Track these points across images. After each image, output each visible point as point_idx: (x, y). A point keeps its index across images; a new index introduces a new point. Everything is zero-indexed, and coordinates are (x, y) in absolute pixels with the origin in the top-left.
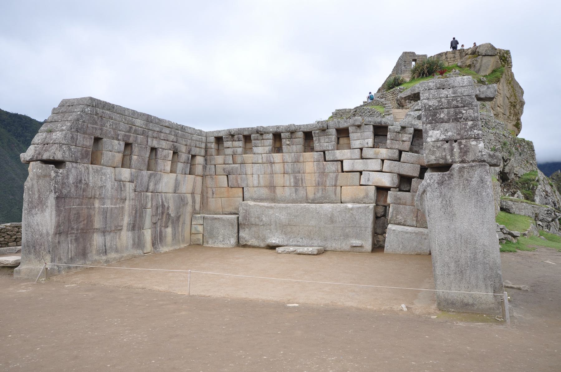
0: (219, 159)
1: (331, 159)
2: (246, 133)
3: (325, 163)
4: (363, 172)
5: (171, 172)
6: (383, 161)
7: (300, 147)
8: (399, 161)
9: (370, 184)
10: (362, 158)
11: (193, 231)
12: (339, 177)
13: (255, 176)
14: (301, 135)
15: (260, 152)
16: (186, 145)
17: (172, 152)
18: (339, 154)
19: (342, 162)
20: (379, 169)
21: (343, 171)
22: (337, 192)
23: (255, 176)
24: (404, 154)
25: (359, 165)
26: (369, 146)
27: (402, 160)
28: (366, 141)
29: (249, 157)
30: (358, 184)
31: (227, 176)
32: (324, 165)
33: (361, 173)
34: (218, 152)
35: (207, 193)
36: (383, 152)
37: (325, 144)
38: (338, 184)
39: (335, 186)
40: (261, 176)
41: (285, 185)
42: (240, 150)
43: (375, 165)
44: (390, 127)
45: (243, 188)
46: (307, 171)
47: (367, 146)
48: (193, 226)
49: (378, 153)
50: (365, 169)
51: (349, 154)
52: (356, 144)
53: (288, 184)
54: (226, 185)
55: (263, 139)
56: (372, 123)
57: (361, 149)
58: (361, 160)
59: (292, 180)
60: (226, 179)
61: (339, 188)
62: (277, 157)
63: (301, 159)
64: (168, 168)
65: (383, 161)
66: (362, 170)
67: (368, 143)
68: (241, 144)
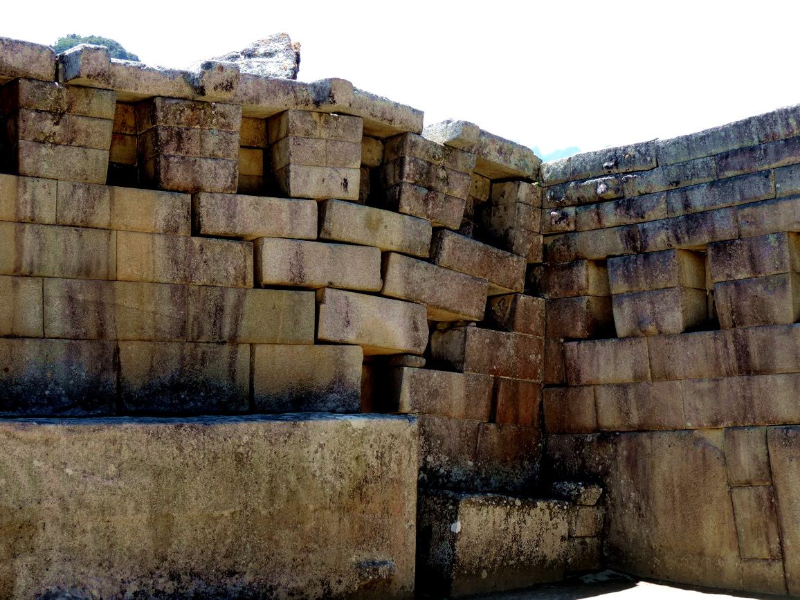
1: (222, 228)
3: (197, 241)
4: (328, 291)
6: (385, 255)
7: (97, 160)
8: (432, 259)
9: (351, 338)
14: (105, 106)
18: (254, 213)
19: (256, 247)
20: (375, 284)
21: (258, 284)
22: (238, 367)
24: (449, 241)
25: (319, 265)
27: (444, 256)
28: (344, 173)
32: (190, 251)
36: (394, 229)
37: (207, 164)
38: (243, 333)
39: (234, 340)
41: (19, 330)
43: (361, 270)
44: (413, 138)
46: (125, 271)
47: (342, 195)
49: (380, 221)
50: (337, 282)
51: (285, 216)
52: (307, 178)
53: (31, 321)
56: (363, 113)
58: (322, 247)
59: (57, 307)
61: (244, 351)
63: (101, 216)
65: (385, 255)
66: (326, 283)
67: (345, 183)
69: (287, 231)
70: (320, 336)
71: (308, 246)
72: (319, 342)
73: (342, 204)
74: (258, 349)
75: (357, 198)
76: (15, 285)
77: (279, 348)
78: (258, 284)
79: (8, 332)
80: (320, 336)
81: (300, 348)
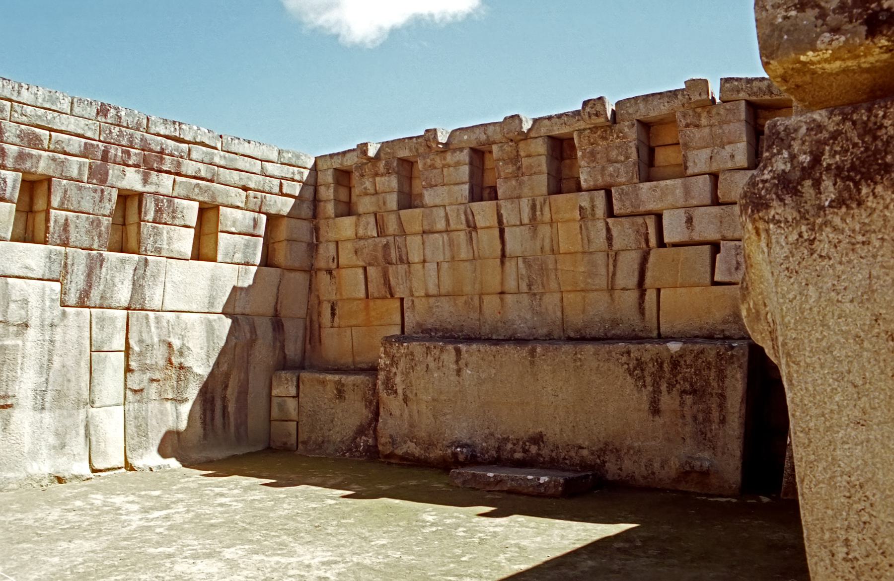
0: (346, 226)
2: (404, 153)
5: (197, 256)
7: (542, 182)
10: (716, 202)
11: (275, 413)
12: (652, 259)
13: (431, 267)
14: (540, 147)
15: (438, 201)
16: (245, 189)
17: (196, 205)
18: (649, 195)
19: (659, 217)
21: (661, 244)
23: (431, 267)
26: (738, 165)
29: (413, 217)
30: (708, 280)
31: (365, 269)
33: (715, 247)
34: (347, 209)
35: (319, 314)
40: (445, 266)
42: (392, 201)
45: (402, 300)
47: (730, 165)
48: (275, 401)
51: (679, 192)
52: (699, 160)
54: (362, 294)
55: (444, 166)
57: (715, 177)
58: (715, 210)
60: (362, 277)
61: (650, 296)
62: (484, 212)
64: (187, 247)
68: (393, 182)
69: (681, 202)
70: (716, 279)
71: (698, 213)
72: (715, 283)
73: (728, 174)
74: (662, 292)
75: (746, 165)
76: (502, 263)
77: (680, 290)
78: (661, 244)
79: (500, 291)
80: (716, 279)
81: (698, 289)
